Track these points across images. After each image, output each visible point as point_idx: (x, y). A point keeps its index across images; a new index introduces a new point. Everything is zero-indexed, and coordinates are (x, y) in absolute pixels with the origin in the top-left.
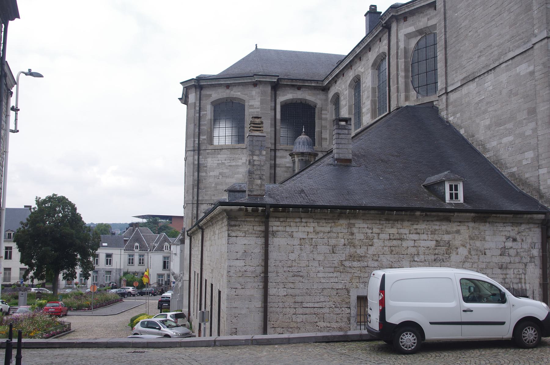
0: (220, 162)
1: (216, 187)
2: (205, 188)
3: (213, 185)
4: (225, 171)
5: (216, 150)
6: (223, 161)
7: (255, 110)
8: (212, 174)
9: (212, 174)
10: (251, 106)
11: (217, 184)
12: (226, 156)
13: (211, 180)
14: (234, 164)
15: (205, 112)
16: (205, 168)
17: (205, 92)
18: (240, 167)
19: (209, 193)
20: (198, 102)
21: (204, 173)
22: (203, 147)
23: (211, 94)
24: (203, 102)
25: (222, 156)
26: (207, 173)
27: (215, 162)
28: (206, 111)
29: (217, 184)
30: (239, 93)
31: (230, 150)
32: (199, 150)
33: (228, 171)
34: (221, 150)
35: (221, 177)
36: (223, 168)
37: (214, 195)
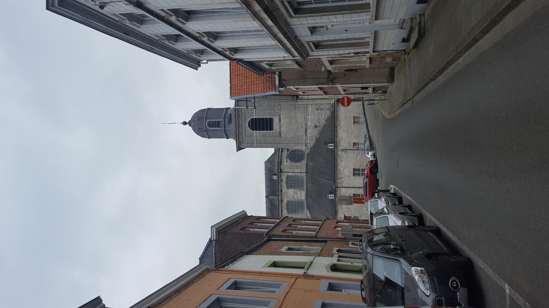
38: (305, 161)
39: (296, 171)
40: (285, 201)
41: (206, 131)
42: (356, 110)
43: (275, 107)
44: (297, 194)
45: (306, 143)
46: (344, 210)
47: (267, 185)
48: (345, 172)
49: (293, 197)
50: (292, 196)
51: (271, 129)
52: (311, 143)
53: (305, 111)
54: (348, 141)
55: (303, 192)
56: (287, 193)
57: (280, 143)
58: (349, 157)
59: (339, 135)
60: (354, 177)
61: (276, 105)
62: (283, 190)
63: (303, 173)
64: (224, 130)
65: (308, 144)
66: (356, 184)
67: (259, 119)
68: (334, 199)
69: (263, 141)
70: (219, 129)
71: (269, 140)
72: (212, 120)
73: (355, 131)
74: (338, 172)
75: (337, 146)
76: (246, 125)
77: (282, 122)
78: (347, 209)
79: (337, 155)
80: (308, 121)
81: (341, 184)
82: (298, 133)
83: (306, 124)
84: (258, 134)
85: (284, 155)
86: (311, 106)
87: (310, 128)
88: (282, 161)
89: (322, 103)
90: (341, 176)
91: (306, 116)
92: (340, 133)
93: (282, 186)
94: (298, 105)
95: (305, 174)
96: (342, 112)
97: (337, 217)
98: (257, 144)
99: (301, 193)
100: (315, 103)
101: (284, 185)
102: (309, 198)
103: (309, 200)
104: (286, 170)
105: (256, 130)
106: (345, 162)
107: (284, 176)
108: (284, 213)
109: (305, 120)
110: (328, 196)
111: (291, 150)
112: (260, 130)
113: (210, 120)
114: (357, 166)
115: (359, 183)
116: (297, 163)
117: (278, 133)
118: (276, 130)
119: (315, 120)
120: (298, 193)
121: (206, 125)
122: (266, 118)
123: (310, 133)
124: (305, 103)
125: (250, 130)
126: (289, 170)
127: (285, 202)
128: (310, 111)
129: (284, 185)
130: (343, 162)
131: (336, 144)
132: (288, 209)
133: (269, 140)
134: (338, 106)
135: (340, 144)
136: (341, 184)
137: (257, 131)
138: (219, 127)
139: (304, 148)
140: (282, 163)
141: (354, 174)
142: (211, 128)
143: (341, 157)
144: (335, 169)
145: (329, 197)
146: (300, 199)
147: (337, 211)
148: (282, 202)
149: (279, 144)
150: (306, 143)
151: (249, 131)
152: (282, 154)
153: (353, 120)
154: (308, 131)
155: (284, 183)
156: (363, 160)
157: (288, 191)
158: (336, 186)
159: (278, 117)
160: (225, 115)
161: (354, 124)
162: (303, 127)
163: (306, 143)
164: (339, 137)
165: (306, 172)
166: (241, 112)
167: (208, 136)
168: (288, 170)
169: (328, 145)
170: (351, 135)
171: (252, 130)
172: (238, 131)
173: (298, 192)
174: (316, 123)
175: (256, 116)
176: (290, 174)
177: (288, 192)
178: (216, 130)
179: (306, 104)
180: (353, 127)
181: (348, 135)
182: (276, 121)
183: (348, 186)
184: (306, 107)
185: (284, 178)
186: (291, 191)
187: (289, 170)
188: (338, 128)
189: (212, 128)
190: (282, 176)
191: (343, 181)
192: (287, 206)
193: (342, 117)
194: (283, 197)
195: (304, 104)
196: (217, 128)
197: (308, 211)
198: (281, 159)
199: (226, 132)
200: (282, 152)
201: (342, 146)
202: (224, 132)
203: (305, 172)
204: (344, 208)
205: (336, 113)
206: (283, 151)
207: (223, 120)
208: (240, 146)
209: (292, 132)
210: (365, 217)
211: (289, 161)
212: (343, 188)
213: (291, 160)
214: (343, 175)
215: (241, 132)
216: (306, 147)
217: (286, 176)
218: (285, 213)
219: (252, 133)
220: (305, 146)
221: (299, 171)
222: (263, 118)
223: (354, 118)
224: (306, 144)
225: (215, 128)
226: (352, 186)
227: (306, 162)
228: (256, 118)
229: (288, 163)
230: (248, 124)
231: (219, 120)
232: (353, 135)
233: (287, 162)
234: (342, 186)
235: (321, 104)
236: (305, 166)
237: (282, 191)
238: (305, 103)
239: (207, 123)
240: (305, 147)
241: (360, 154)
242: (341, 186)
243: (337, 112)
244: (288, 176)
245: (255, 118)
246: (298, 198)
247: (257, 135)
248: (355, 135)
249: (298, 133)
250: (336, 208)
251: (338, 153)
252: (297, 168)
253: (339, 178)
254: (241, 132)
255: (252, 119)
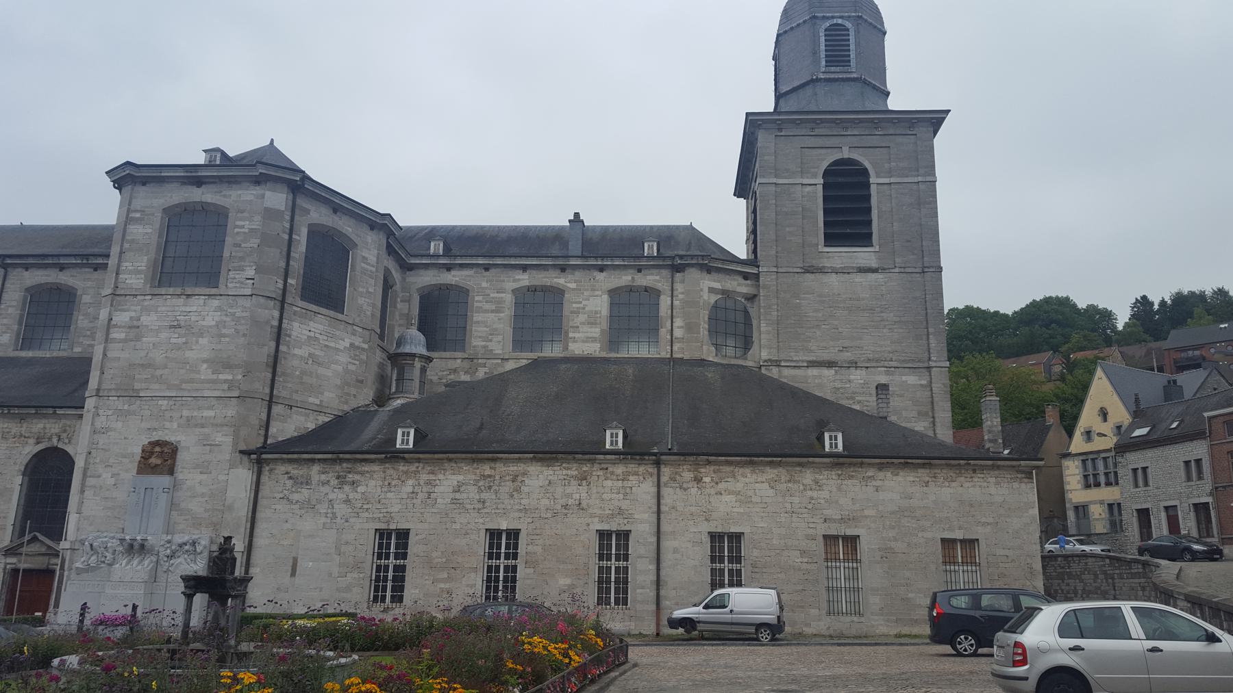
0: (312, 334)
1: (302, 378)
2: (284, 374)
3: (297, 373)
4: (318, 353)
5: (308, 312)
6: (317, 335)
7: (368, 267)
8: (297, 351)
9: (297, 351)
10: (364, 257)
11: (303, 373)
12: (321, 327)
13: (295, 363)
14: (332, 344)
15: (298, 238)
16: (288, 339)
17: (302, 202)
18: (340, 353)
19: (290, 385)
20: (289, 213)
21: (286, 347)
22: (289, 299)
23: (310, 210)
24: (297, 218)
25: (316, 325)
26: (289, 348)
27: (304, 332)
28: (299, 235)
29: (303, 373)
30: (350, 230)
31: (328, 318)
32: (283, 302)
33: (322, 354)
34: (316, 314)
35: (310, 362)
36: (316, 347)
37: (297, 392)
38: (713, 357)
39: (678, 322)
40: (561, 281)
41: (814, 17)
42: (1007, 552)
43: (913, 254)
44: (588, 324)
45: (780, 361)
46: (560, 490)
47: (611, 230)
48: (727, 498)
49: (577, 312)
50: (581, 306)
51: (832, 239)
52: (787, 375)
53: (909, 361)
54: (866, 512)
55: (597, 346)
56: (593, 290)
57: (780, 270)
58: (794, 519)
59: (889, 474)
60: (706, 540)
61: (923, 257)
62: (604, 274)
63: (669, 348)
64: (818, 80)
65: (779, 371)
66: (675, 544)
67: (868, 198)
68: (602, 450)
69: (785, 209)
70: (820, 62)
71: (787, 229)
72: (852, 38)
73: (909, 545)
74: (728, 469)
75: (843, 464)
76: (845, 149)
77: (859, 278)
78: (563, 501)
79: (800, 465)
80: (864, 372)
81: (673, 479)
82: (818, 333)
83: (854, 365)
84: (808, 193)
85: (735, 283)
86: (924, 382)
87: (838, 377)
88: (715, 275)
89: (938, 424)
90: (707, 479)
91: (886, 364)
92: (900, 478)
93: (617, 272)
94: (925, 337)
95: (665, 354)
96: (993, 490)
97: (527, 459)
98: (773, 188)
99: (594, 340)
100: (936, 399)
101: (625, 279)
102: (576, 367)
103: (569, 365)
104: (679, 287)
105: (825, 186)
106: (768, 500)
107: (658, 278)
108: (517, 277)
109: (869, 360)
110: (616, 427)
111: (750, 310)
112: (825, 198)
113: (852, 33)
114: (756, 553)
115: (678, 556)
116: (707, 326)
117: (814, 262)
118: (829, 257)
119: (868, 398)
120: (593, 330)
121: (833, 17)
122: (869, 223)
123: (820, 377)
124: (935, 361)
125: (825, 165)
126: (681, 296)
127: (560, 280)
128: (904, 378)
129: (625, 279)
130: (771, 492)
131: (850, 464)
132: (533, 289)
133: (787, 229)
134: (1019, 476)
135: (851, 477)
136: (673, 479)
137: (820, 188)
138: (826, 61)
139: (765, 355)
140: (705, 274)
141: (715, 537)
142: (822, 34)
143: (789, 481)
144: (745, 456)
145: (611, 428)
146: (571, 335)
147: (557, 460)
148: (558, 271)
149: (777, 267)
150: (783, 364)
151: (824, 160)
152: (737, 277)
153: (959, 535)
154: (828, 373)
155: (630, 278)
156: (782, 576)
157: (600, 293)
158: (663, 457)
159: (874, 265)
160: (869, 84)
161: (943, 540)
162: (841, 354)
163: (780, 361)
164: (881, 475)
165: (672, 361)
166: (891, 132)
167: (792, 28)
168: (682, 293)
169: (837, 430)
170: (893, 528)
171: (827, 174)
172: (822, 121)
173: (598, 330)
174: (859, 402)
175: (880, 187)
176: (665, 301)
177: (597, 293)
178: (815, 53)
179: (932, 364)
180: (929, 535)
181: (893, 513)
182: (863, 256)
183: (663, 508)
184: (921, 365)
185: (649, 277)
186: (600, 304)
187: (681, 296)
188: (919, 470)
189: (823, 39)
190: (655, 271)
191: (685, 490)
192: (545, 289)
193: (971, 490)
194: (578, 274)
195: (930, 359)
196: (823, 55)
197: (524, 362)
198: (719, 270)
199: (807, 87)
200: (746, 276)
201: (839, 489)
202: (809, 79)
203: (674, 356)
204: (569, 490)
205: (990, 463)
206: (748, 282)
207: (855, 75)
208: (764, 126)
209: (820, 315)
210: (528, 582)
211: (714, 298)
212: (654, 490)
213: (715, 307)
214: (713, 491)
215: (817, 132)
216: (765, 361)
217: (659, 286)
218: (515, 281)
219: (813, 170)
220: (770, 360)
221: (678, 333)
222: (869, 210)
223: (970, 544)
224: (777, 361)
225: (823, 48)
226: (665, 527)
227: (711, 359)
228: (867, 185)
229: (705, 295)
230: (846, 156)
231: (853, 63)
232: (892, 534)
233: (711, 290)
234: (666, 485)
235: (934, 423)
236: (697, 355)
237: (601, 269)
238: (935, 361)
239: (840, 21)
240: (767, 358)
241: (809, 566)
242: (664, 479)
243: (993, 467)
244: (658, 293)
245: (872, 180)
246: (572, 327)
247: (809, 189)
248: (893, 544)
249: (818, 333)
250: (570, 457)
251: (808, 472)
252: (690, 328)
253: (696, 470)
254: (817, 132)
255: (865, 172)
